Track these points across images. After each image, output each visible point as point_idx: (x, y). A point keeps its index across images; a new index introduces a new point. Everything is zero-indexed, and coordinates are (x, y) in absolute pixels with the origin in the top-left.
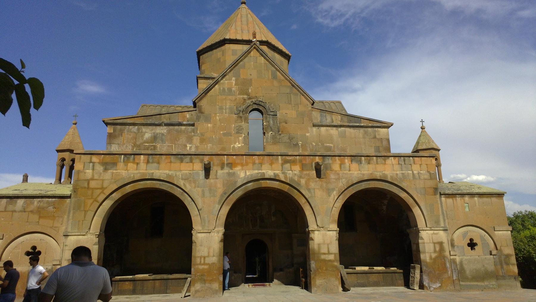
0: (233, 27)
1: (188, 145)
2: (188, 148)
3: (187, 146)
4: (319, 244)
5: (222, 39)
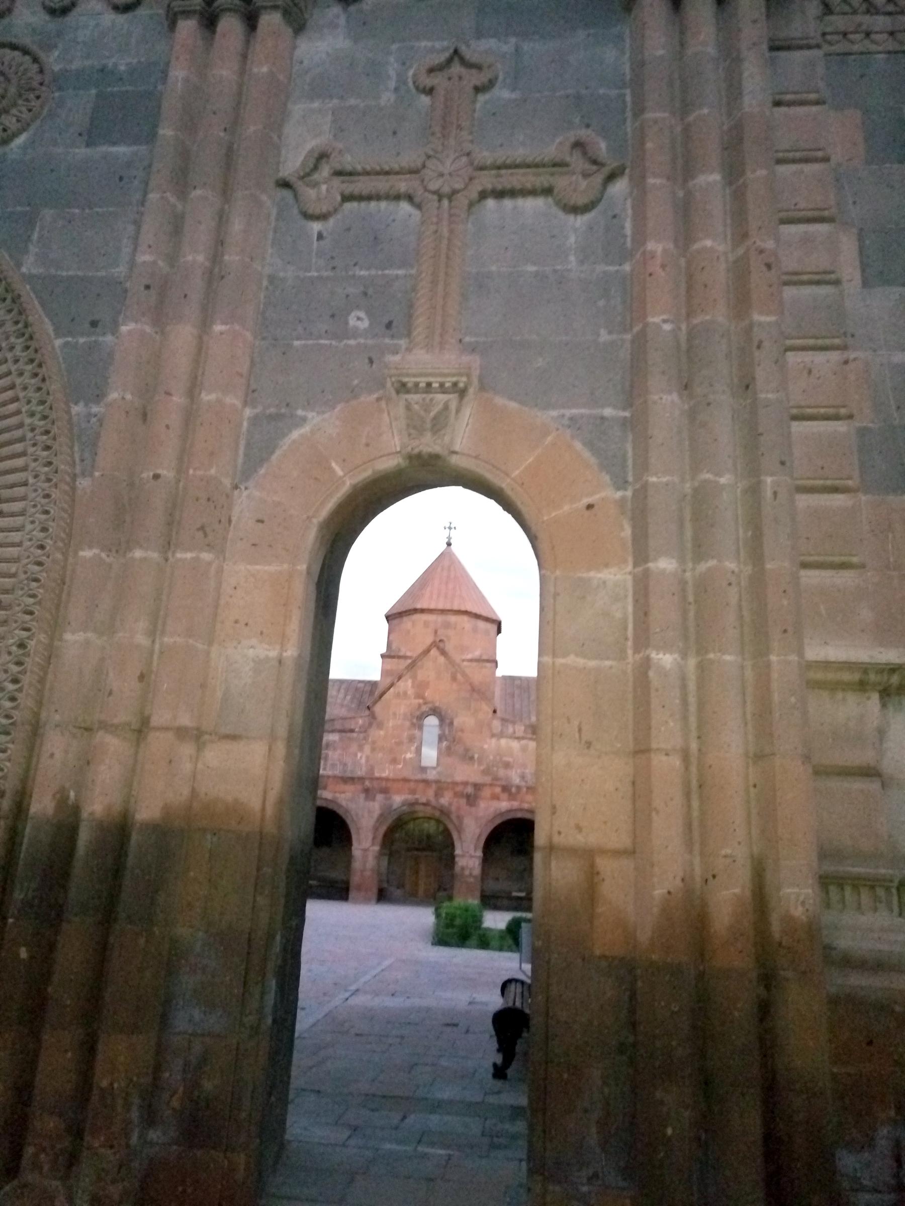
0: (429, 589)
1: (359, 755)
2: (359, 758)
3: (356, 755)
4: (463, 869)
5: (411, 607)
